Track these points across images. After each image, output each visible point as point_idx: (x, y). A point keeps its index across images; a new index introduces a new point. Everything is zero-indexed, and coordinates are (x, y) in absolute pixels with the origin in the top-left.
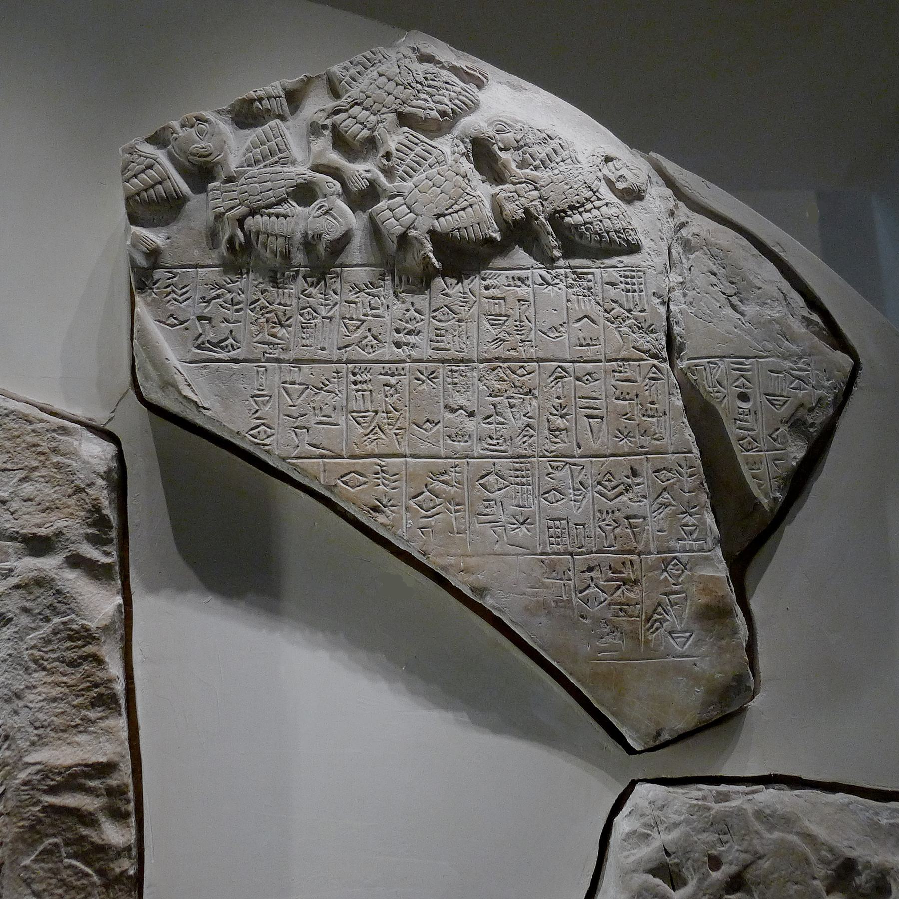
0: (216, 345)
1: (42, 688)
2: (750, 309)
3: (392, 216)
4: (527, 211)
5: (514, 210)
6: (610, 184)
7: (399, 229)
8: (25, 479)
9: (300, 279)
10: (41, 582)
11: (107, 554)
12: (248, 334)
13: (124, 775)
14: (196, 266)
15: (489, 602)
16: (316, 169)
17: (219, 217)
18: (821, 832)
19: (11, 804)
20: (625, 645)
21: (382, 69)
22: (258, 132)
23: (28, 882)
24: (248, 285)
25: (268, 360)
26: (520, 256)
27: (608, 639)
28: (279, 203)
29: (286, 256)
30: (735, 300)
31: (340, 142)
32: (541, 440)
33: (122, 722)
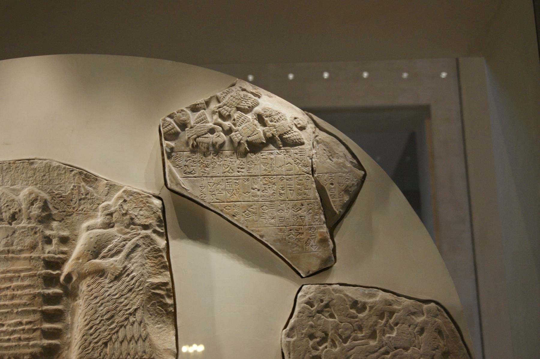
0: (190, 173)
1: (149, 263)
2: (335, 160)
3: (236, 137)
4: (273, 134)
5: (269, 134)
6: (296, 125)
7: (238, 140)
8: (140, 210)
9: (212, 155)
10: (147, 237)
11: (162, 230)
12: (198, 170)
13: (170, 286)
14: (183, 152)
15: (263, 240)
16: (215, 124)
17: (189, 138)
18: (350, 295)
19: (145, 291)
20: (300, 249)
21: (232, 94)
22: (199, 113)
23: (149, 311)
24: (198, 156)
25: (204, 177)
26: (271, 147)
27: (295, 248)
28: (206, 134)
29: (208, 148)
30: (331, 157)
31: (221, 116)
32: (277, 196)
33: (168, 273)
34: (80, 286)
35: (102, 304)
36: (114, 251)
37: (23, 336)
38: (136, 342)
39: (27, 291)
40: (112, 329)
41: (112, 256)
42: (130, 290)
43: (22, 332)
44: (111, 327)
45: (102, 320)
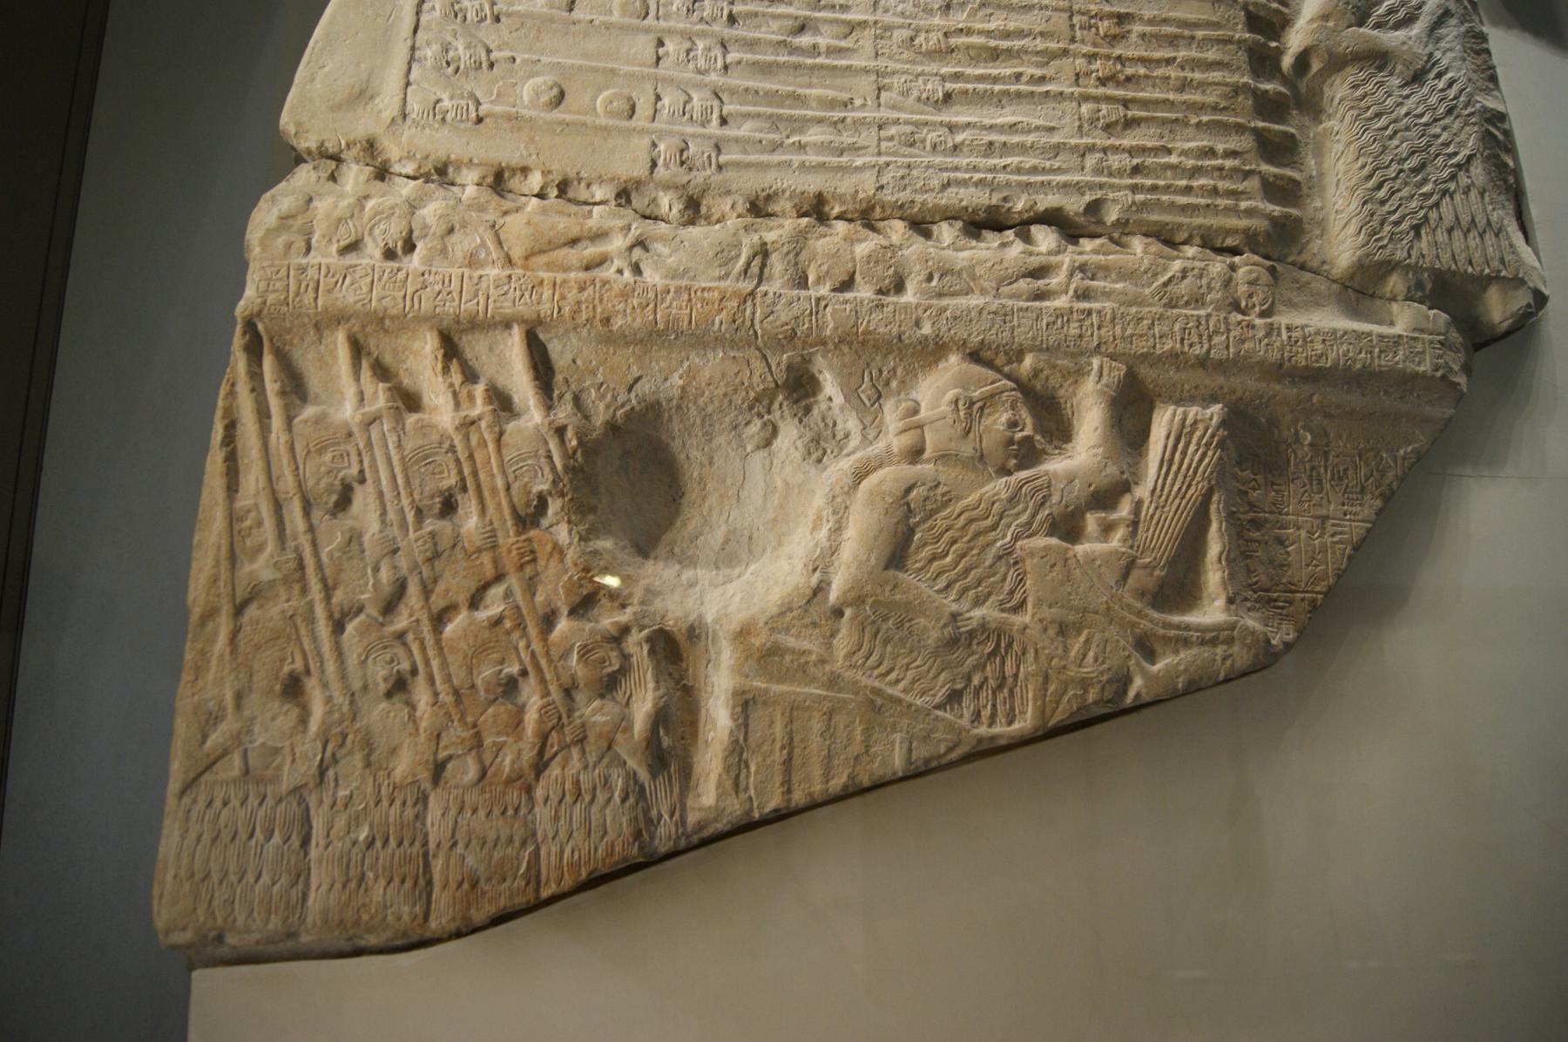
34: (1326, 90)
35: (1395, 133)
36: (1401, 14)
37: (1222, 185)
38: (1481, 236)
39: (1216, 75)
40: (1428, 196)
41: (1397, 27)
42: (1450, 111)
43: (1216, 174)
44: (1425, 189)
45: (1401, 171)
